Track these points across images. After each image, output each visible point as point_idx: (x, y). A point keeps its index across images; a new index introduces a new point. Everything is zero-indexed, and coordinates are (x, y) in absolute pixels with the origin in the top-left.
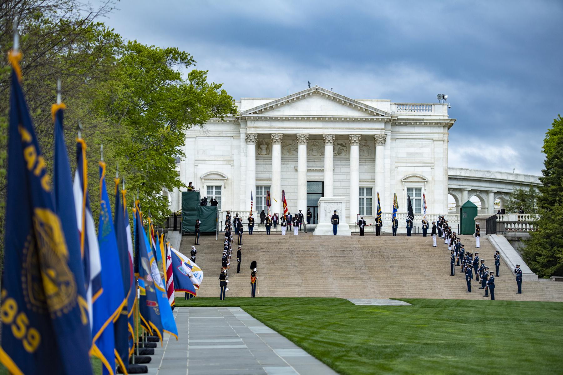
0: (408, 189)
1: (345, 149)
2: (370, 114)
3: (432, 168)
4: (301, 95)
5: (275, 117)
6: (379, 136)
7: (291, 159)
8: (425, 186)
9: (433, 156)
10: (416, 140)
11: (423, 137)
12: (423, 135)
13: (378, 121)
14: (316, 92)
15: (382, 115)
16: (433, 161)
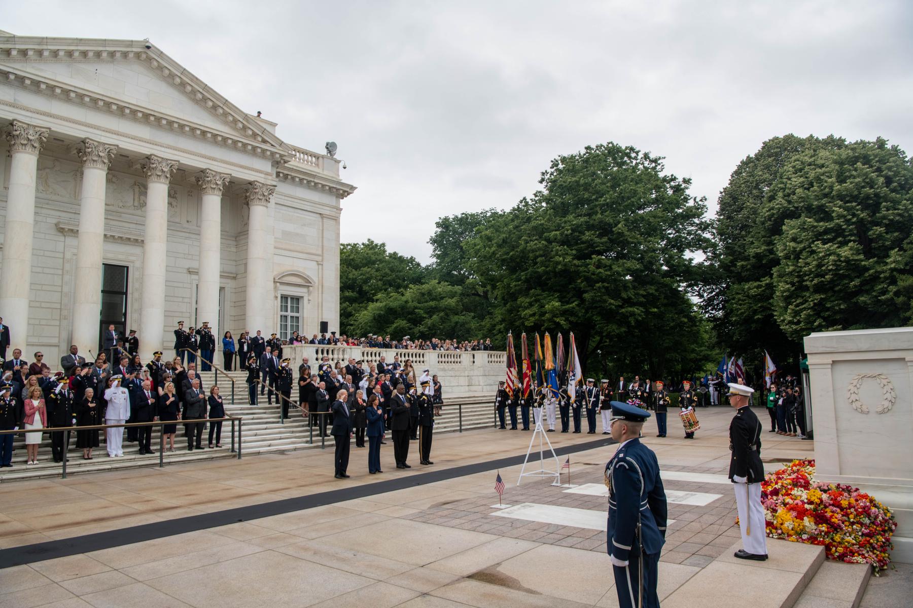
0: (284, 298)
1: (174, 204)
2: (247, 136)
3: (318, 264)
4: (108, 49)
5: (33, 81)
6: (261, 185)
7: (47, 204)
8: (309, 293)
9: (321, 244)
10: (296, 210)
11: (309, 207)
12: (309, 204)
13: (263, 154)
14: (144, 56)
15: (272, 145)
16: (320, 252)
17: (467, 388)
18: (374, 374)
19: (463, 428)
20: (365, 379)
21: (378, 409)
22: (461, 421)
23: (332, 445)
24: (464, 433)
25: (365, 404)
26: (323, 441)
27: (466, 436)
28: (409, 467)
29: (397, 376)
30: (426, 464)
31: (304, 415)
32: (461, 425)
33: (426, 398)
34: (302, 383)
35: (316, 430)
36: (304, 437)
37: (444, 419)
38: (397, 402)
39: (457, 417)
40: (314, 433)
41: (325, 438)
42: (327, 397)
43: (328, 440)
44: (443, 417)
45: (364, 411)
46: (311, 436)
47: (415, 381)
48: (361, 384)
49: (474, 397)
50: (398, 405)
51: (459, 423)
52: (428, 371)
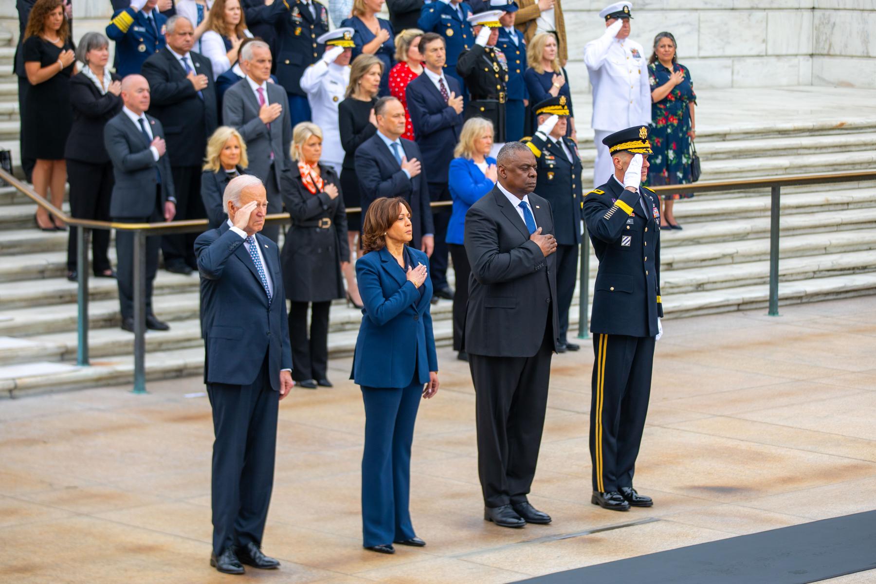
17: (805, 66)
18: (372, 25)
19: (784, 289)
20: (331, 54)
21: (410, 261)
22: (775, 255)
23: (180, 373)
24: (787, 315)
25: (332, 191)
26: (140, 350)
27: (798, 339)
28: (544, 521)
29: (483, 38)
30: (623, 509)
31: (43, 221)
32: (775, 278)
33: (629, 210)
34: (37, 72)
35: (105, 296)
36: (52, 329)
37: (696, 241)
38: (499, 230)
39: (757, 234)
40: (96, 309)
41: (151, 336)
42: (157, 149)
43: (160, 347)
44: (690, 231)
45: (327, 223)
46: (85, 324)
47: (563, 55)
48: (310, 78)
49: (841, 128)
50: (504, 247)
51: (764, 268)
52: (624, 15)
